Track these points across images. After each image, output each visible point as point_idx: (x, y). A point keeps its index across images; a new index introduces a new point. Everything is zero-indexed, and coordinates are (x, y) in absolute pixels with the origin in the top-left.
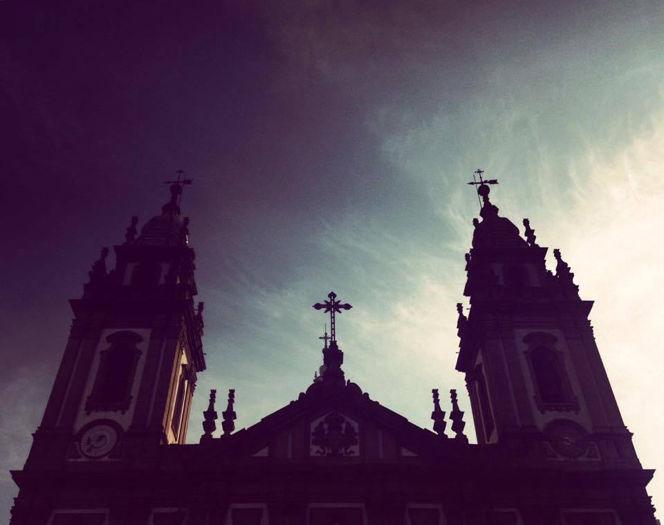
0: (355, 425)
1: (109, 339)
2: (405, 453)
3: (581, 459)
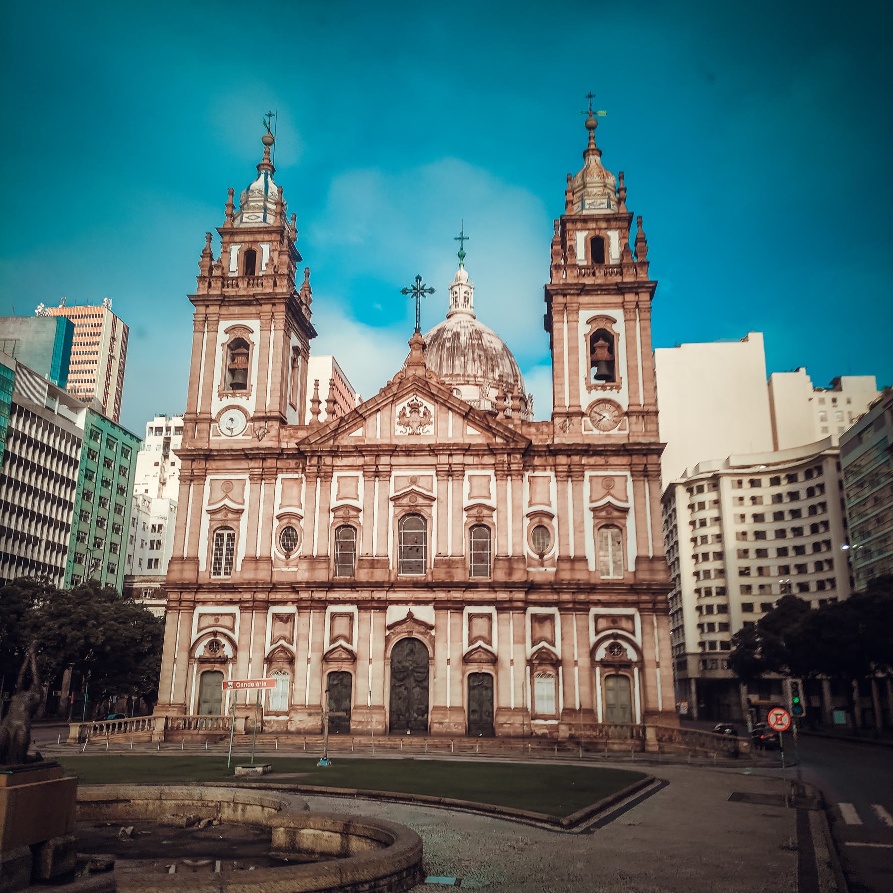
1: (226, 332)
2: (471, 430)
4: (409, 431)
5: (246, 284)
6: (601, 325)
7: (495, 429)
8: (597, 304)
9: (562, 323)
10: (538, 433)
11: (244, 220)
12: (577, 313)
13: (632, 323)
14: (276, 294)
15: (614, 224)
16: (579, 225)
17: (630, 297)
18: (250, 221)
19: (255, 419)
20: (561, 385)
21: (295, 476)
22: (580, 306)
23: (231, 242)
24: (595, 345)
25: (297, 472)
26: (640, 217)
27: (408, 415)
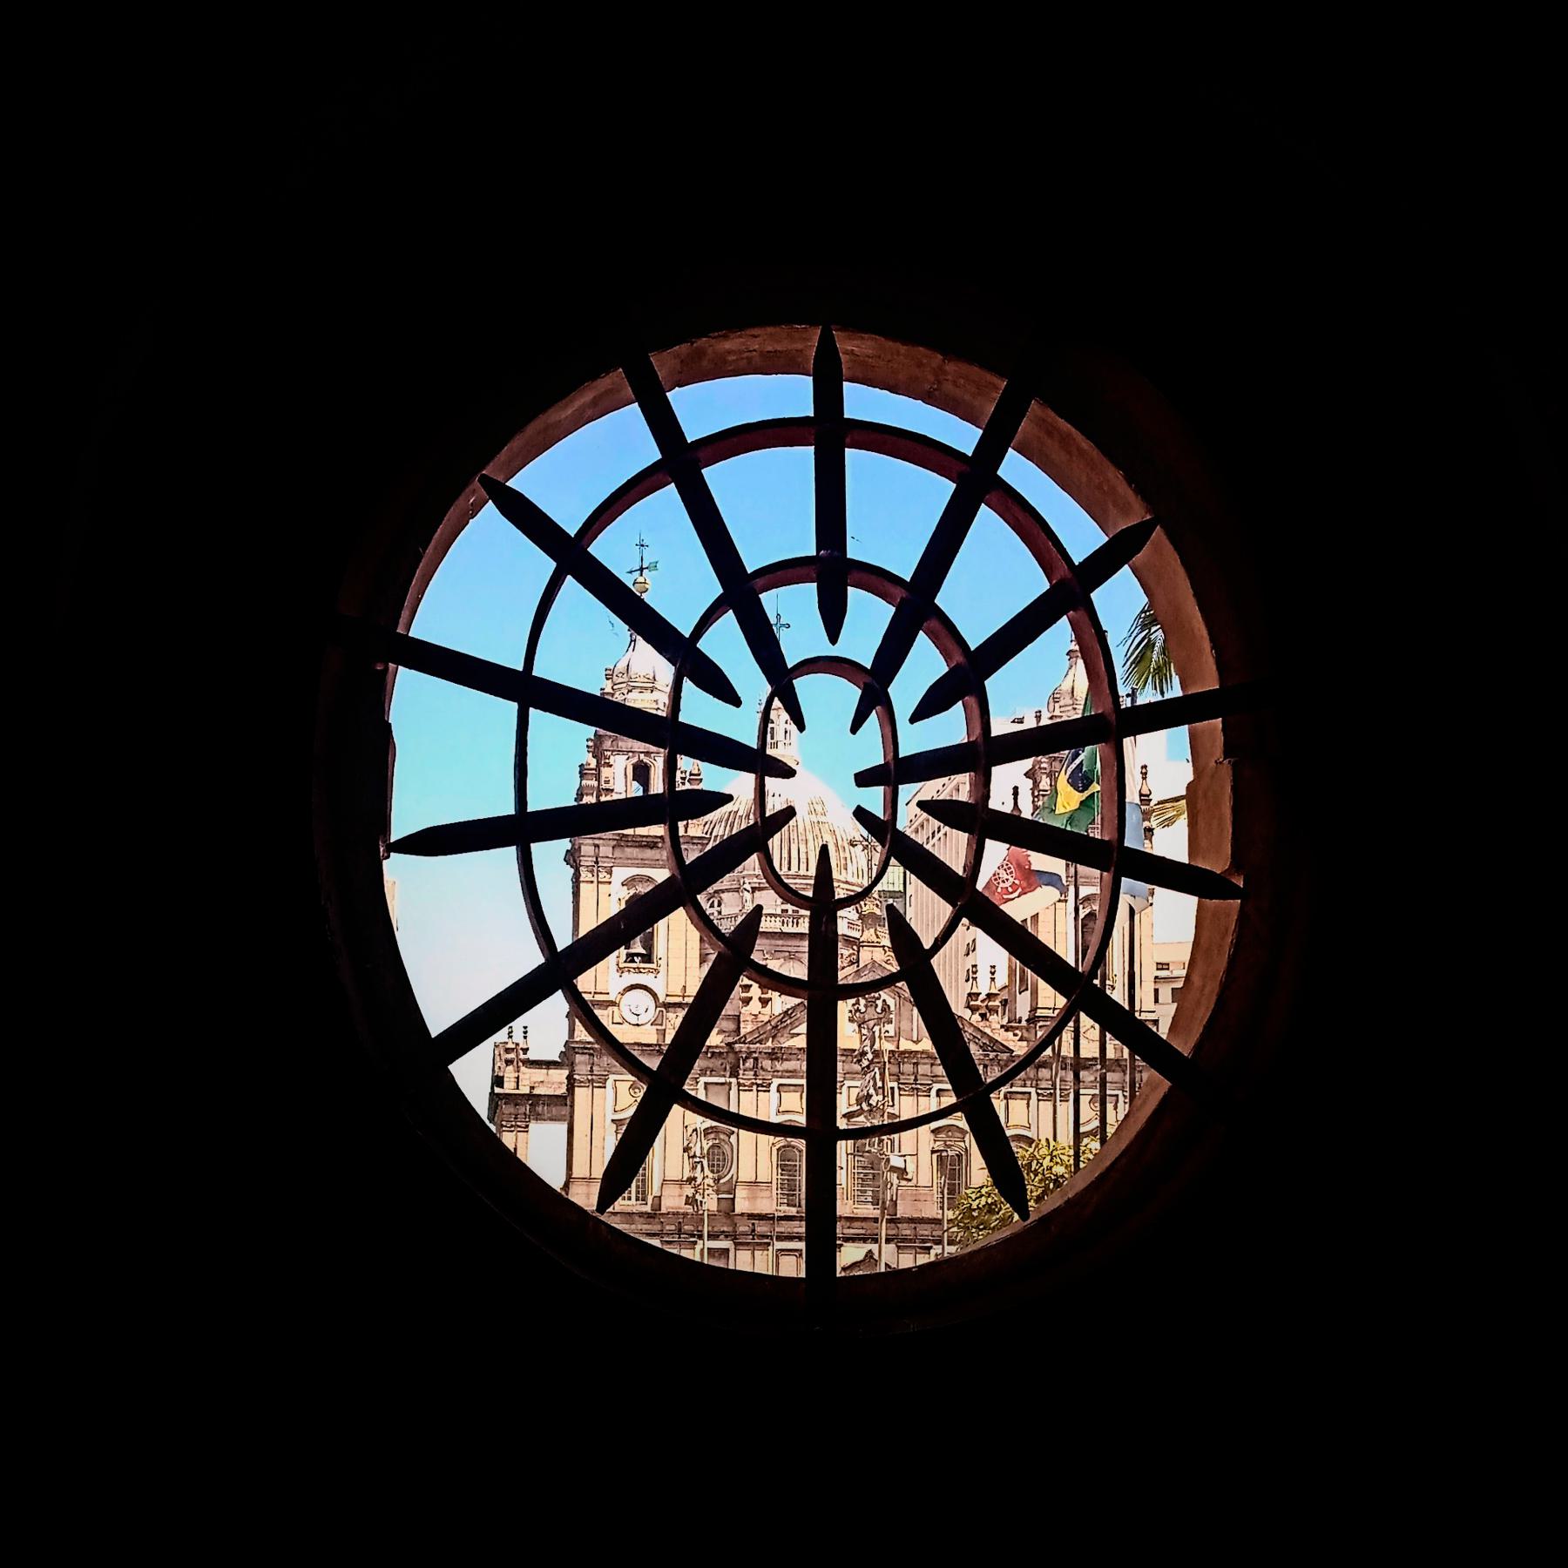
0: (891, 1002)
21: (722, 1080)
25: (724, 1076)
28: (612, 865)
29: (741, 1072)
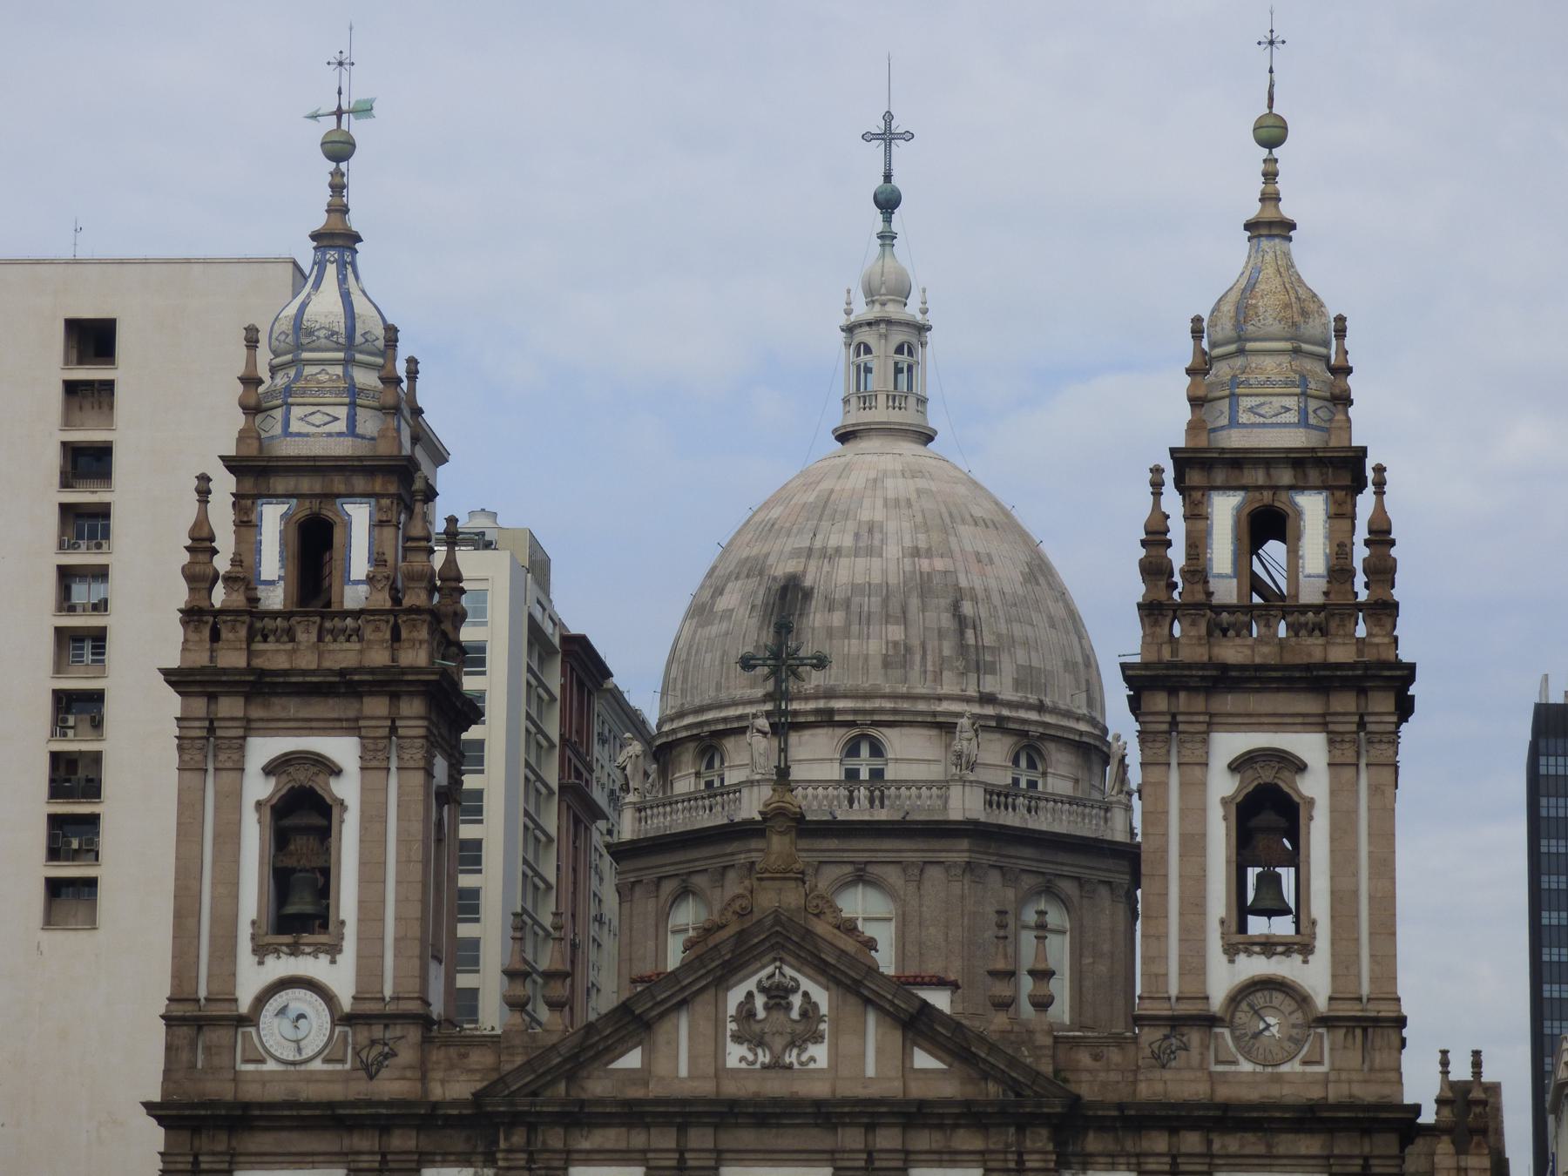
1: (270, 770)
2: (923, 1060)
3: (1285, 1068)
4: (764, 1057)
5: (314, 637)
6: (1267, 776)
7: (985, 1061)
8: (1260, 715)
9: (1164, 768)
10: (1097, 1065)
11: (295, 426)
12: (1205, 742)
13: (1349, 773)
14: (404, 671)
15: (1314, 476)
16: (1220, 477)
17: (1345, 703)
18: (312, 430)
19: (349, 1020)
20: (1158, 938)
22: (1214, 722)
23: (260, 496)
24: (1255, 822)
26: (1379, 470)
27: (761, 1014)
28: (240, 732)
29: (500, 1156)
